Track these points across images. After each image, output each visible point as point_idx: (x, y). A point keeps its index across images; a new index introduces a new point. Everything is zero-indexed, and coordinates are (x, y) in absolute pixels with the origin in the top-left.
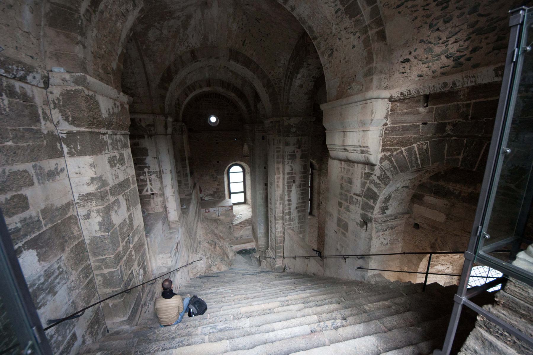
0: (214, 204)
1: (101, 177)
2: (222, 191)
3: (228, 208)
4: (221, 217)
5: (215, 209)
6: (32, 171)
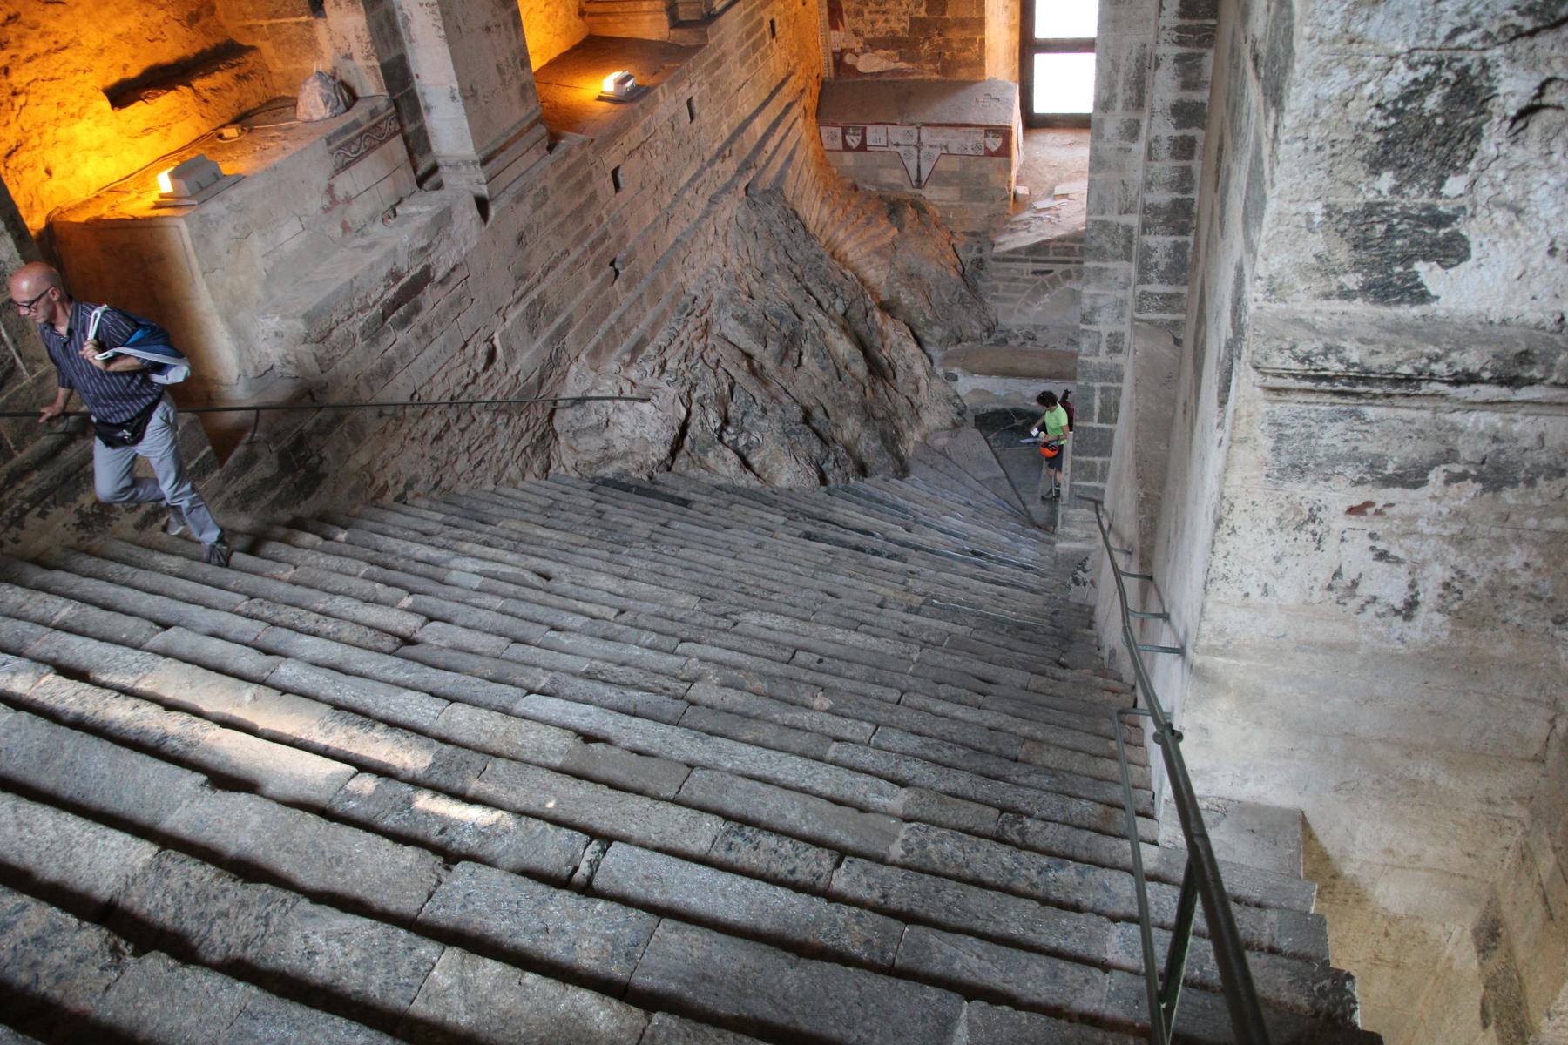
0: (898, 98)
2: (963, 24)
3: (979, 137)
4: (931, 194)
5: (897, 133)
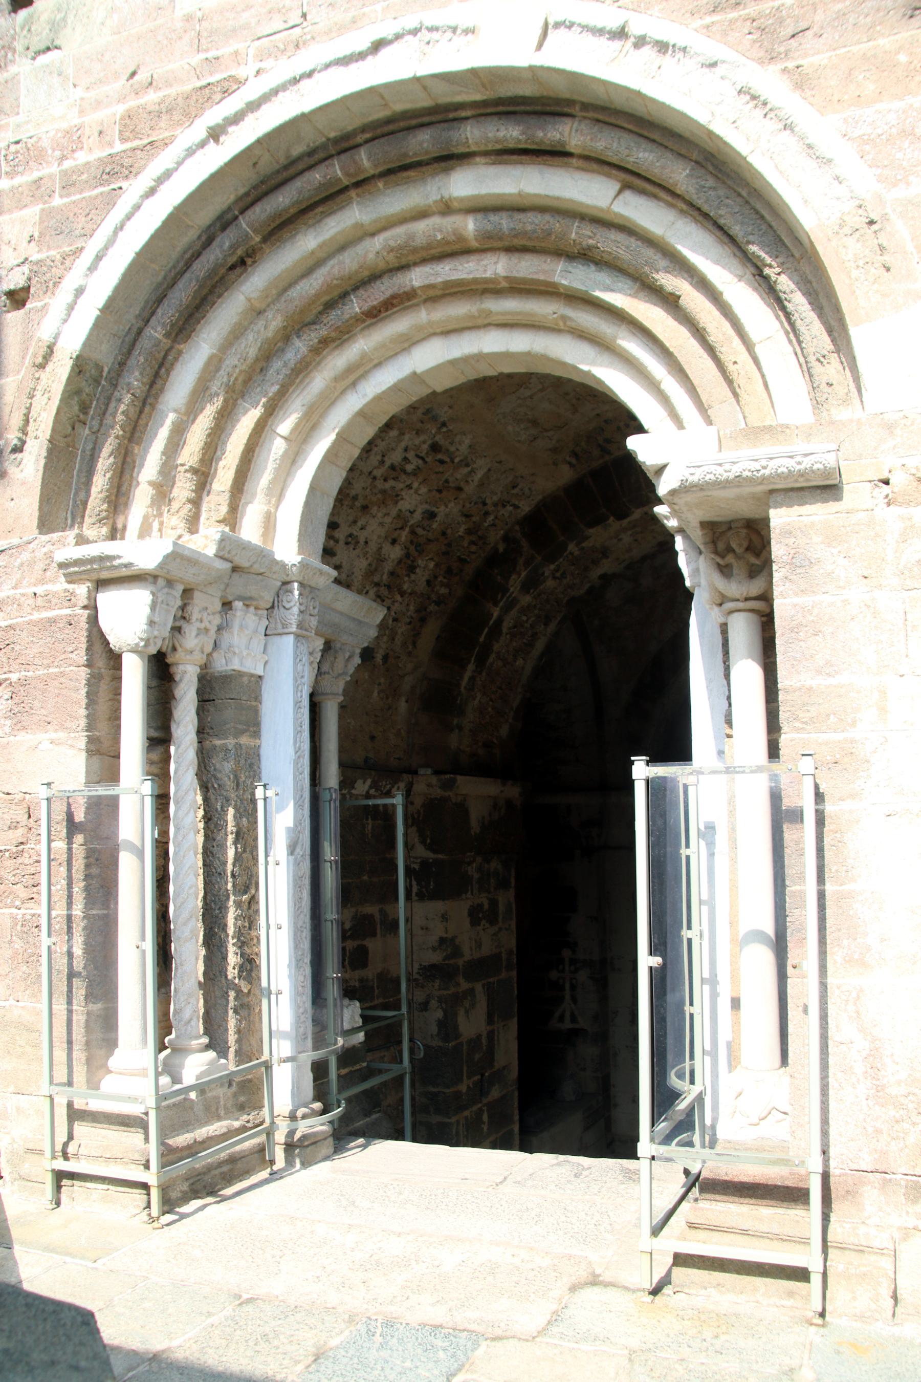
1: (453, 939)
6: (377, 917)
